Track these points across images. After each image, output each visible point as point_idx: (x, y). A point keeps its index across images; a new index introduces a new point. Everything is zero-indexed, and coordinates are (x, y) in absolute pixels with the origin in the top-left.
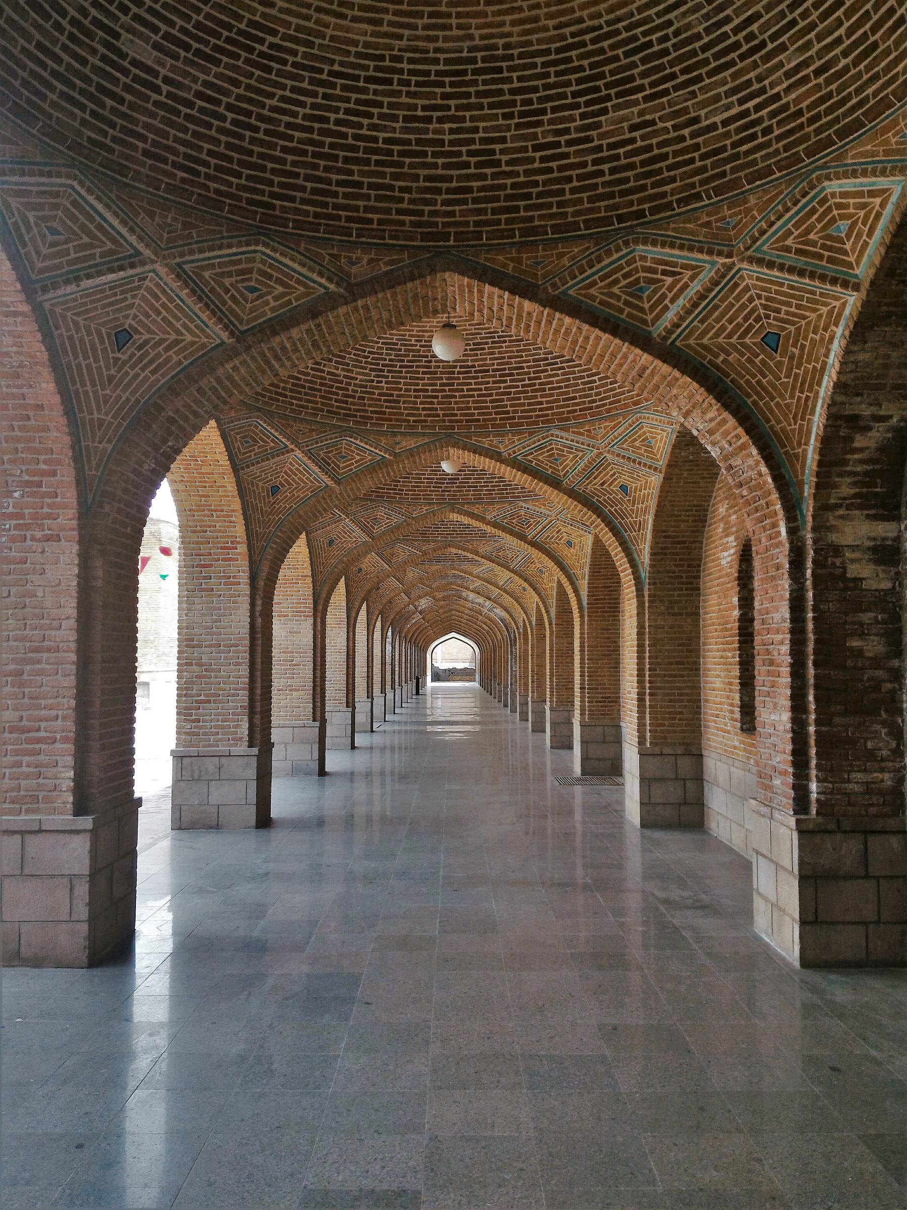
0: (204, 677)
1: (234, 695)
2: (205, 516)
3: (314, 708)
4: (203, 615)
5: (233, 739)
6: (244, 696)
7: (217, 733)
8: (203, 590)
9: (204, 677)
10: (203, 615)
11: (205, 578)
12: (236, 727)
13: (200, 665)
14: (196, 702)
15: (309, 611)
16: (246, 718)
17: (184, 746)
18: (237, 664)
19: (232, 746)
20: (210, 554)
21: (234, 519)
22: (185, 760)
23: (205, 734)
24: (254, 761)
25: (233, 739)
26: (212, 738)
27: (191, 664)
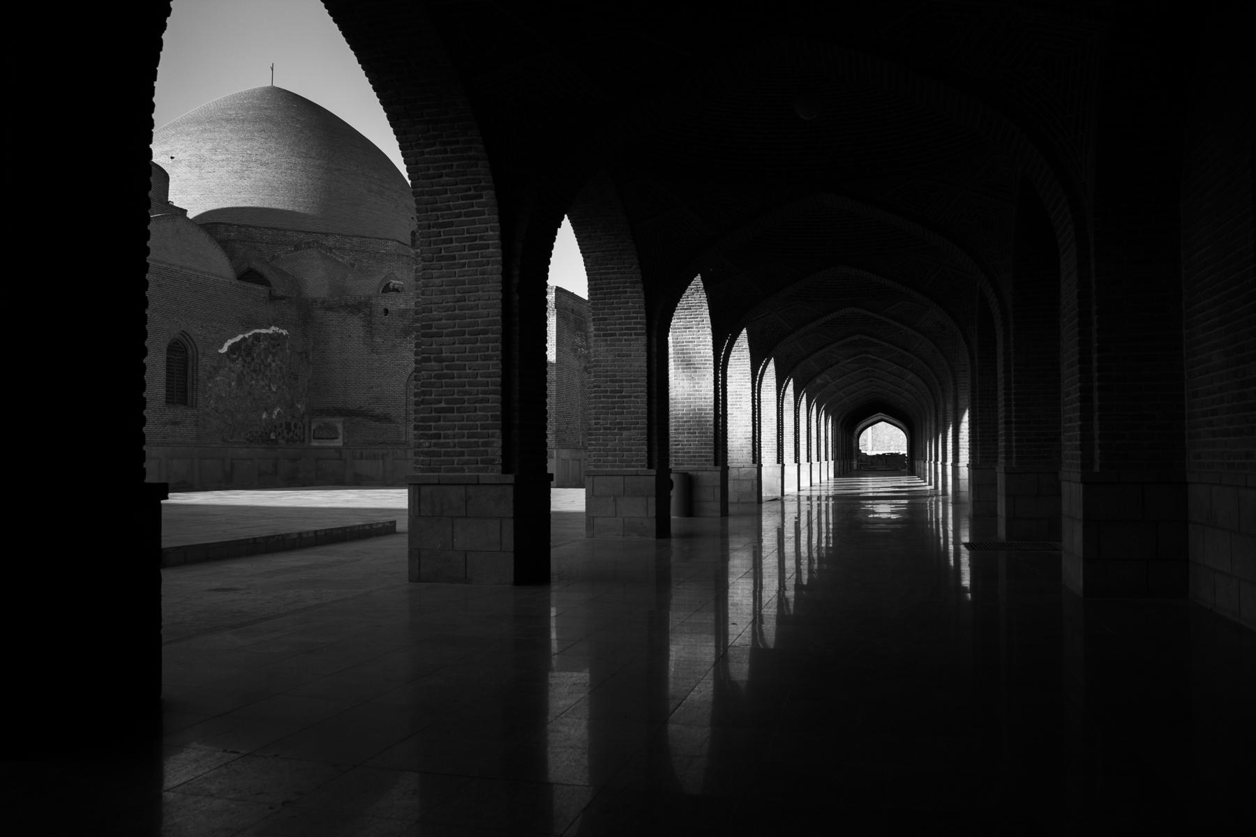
0: (445, 376)
1: (482, 401)
2: (436, 153)
3: (650, 451)
4: (442, 292)
5: (483, 462)
6: (495, 401)
7: (462, 454)
8: (441, 259)
9: (445, 376)
10: (442, 292)
11: (444, 241)
12: (486, 444)
13: (440, 360)
14: (437, 410)
15: (641, 328)
16: (498, 432)
17: (423, 471)
18: (486, 358)
19: (481, 470)
20: (449, 208)
21: (472, 153)
22: (426, 490)
23: (447, 454)
24: (510, 491)
25: (483, 462)
26: (456, 459)
27: (428, 360)
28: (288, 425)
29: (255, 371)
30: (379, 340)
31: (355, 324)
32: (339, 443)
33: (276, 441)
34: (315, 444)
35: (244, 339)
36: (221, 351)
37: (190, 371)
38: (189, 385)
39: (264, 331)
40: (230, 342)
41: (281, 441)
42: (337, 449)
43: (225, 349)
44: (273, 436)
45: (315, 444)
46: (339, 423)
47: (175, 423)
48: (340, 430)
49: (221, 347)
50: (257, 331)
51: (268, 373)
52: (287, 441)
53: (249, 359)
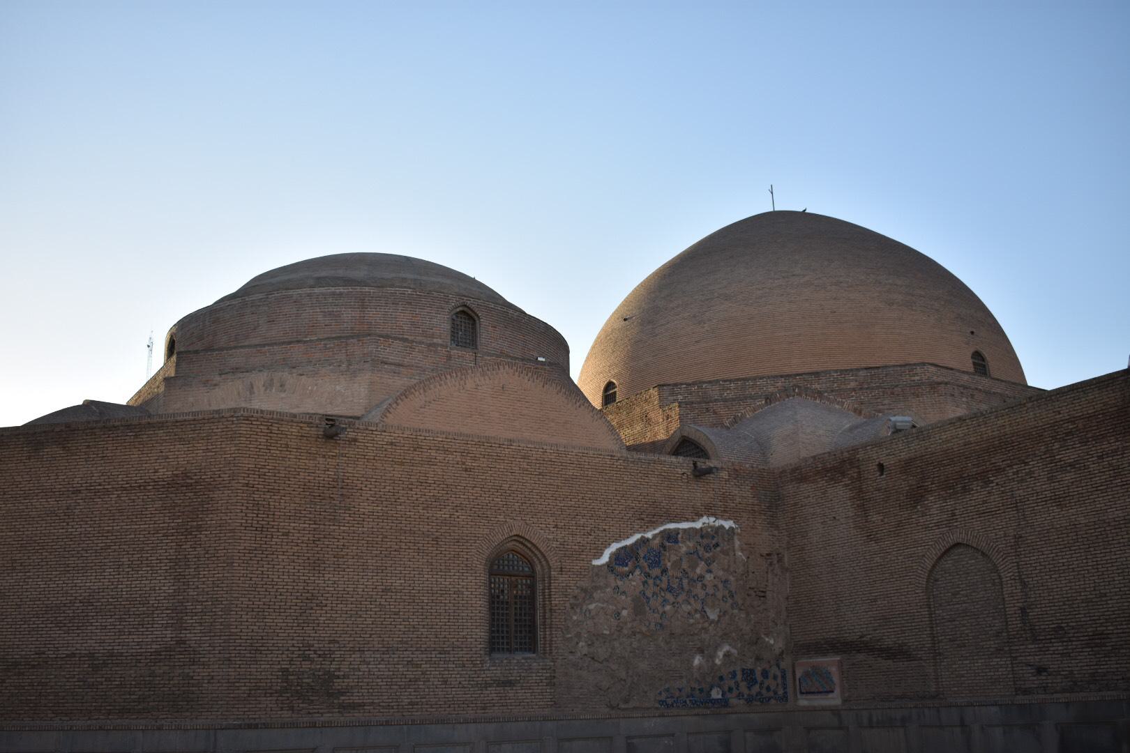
28: (749, 675)
29: (670, 589)
30: (876, 518)
31: (840, 494)
32: (834, 700)
33: (724, 703)
34: (803, 702)
35: (644, 541)
36: (597, 562)
37: (539, 599)
38: (539, 621)
39: (685, 525)
40: (614, 547)
41: (734, 701)
42: (835, 711)
43: (605, 559)
44: (716, 694)
45: (803, 702)
46: (830, 663)
47: (510, 683)
48: (836, 679)
49: (599, 555)
50: (672, 526)
51: (698, 590)
52: (749, 700)
53: (656, 572)
